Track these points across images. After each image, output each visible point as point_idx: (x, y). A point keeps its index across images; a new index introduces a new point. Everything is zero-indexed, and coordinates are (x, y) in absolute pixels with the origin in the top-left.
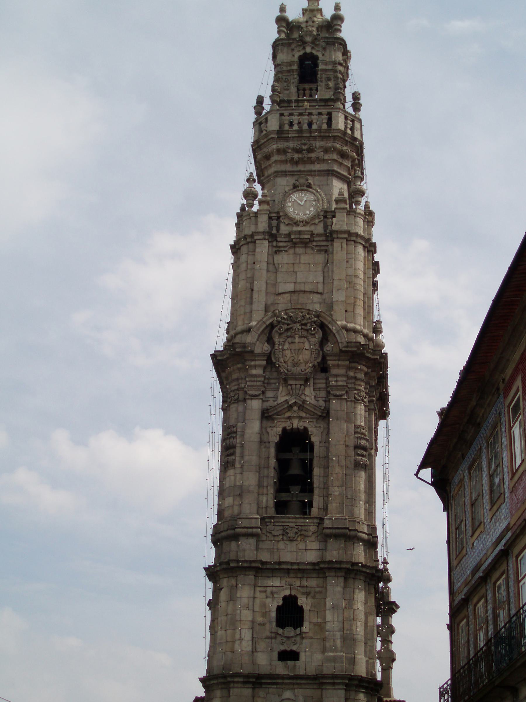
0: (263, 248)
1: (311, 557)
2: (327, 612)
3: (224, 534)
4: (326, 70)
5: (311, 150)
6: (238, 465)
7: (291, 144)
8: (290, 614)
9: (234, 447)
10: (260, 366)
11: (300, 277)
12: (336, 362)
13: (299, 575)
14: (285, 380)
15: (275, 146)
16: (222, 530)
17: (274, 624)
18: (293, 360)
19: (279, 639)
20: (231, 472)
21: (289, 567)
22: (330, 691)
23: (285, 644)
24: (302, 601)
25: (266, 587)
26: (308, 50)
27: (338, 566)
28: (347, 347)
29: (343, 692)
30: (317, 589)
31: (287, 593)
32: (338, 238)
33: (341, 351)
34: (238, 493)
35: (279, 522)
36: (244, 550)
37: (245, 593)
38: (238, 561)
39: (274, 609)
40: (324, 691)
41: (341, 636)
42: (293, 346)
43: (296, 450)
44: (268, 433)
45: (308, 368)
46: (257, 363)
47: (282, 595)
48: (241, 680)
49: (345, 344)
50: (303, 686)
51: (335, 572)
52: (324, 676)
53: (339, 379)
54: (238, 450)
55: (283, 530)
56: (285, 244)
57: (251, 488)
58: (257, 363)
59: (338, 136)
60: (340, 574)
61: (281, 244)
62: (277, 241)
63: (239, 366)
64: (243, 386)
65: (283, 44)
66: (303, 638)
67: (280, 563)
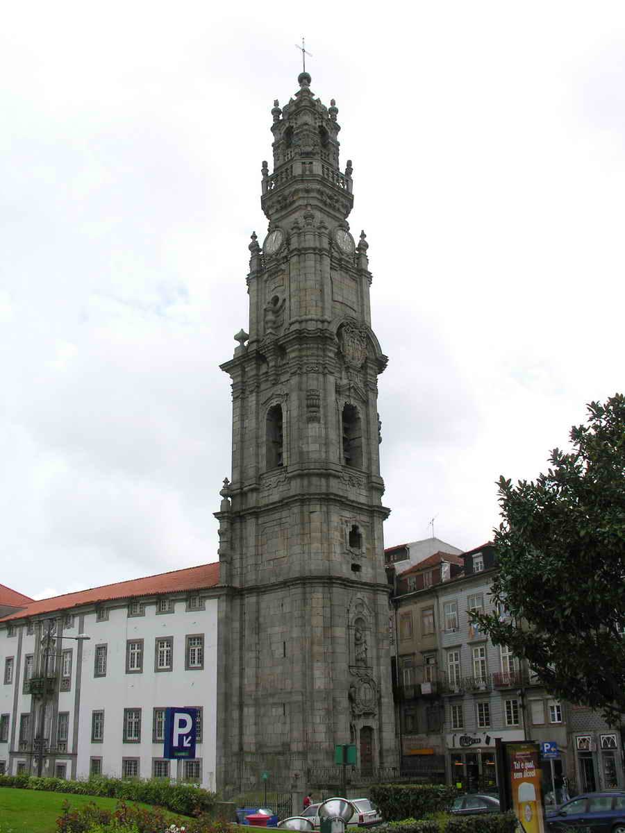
0: (327, 261)
1: (363, 500)
5: (337, 201)
6: (322, 422)
7: (327, 191)
9: (319, 407)
10: (334, 352)
12: (372, 366)
14: (347, 368)
15: (318, 187)
16: (312, 467)
20: (316, 425)
21: (357, 505)
24: (361, 530)
26: (324, 124)
31: (354, 524)
33: (377, 359)
37: (335, 519)
39: (348, 533)
45: (358, 363)
55: (350, 477)
57: (334, 441)
60: (381, 516)
61: (334, 264)
64: (321, 362)
65: (310, 111)
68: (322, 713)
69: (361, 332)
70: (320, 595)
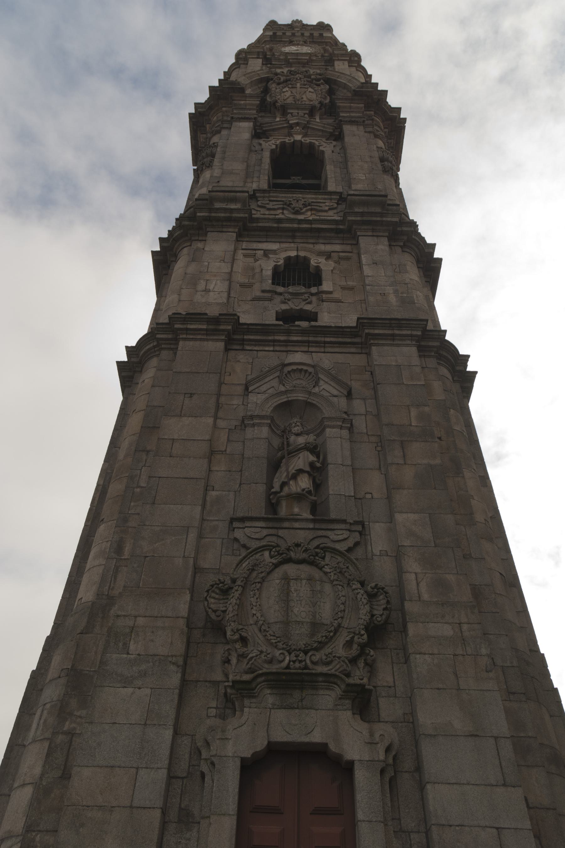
2: (365, 268)
8: (296, 274)
17: (270, 281)
18: (294, 98)
19: (278, 299)
20: (207, 175)
21: (296, 226)
22: (386, 348)
23: (290, 303)
25: (255, 250)
28: (362, 87)
29: (414, 349)
30: (341, 254)
31: (293, 254)
32: (338, 60)
34: (217, 181)
35: (277, 197)
40: (374, 348)
41: (396, 292)
42: (294, 91)
44: (260, 144)
46: (247, 102)
47: (284, 255)
48: (205, 327)
50: (327, 350)
51: (373, 230)
52: (372, 322)
54: (218, 156)
59: (330, 42)
62: (271, 64)
66: (323, 301)
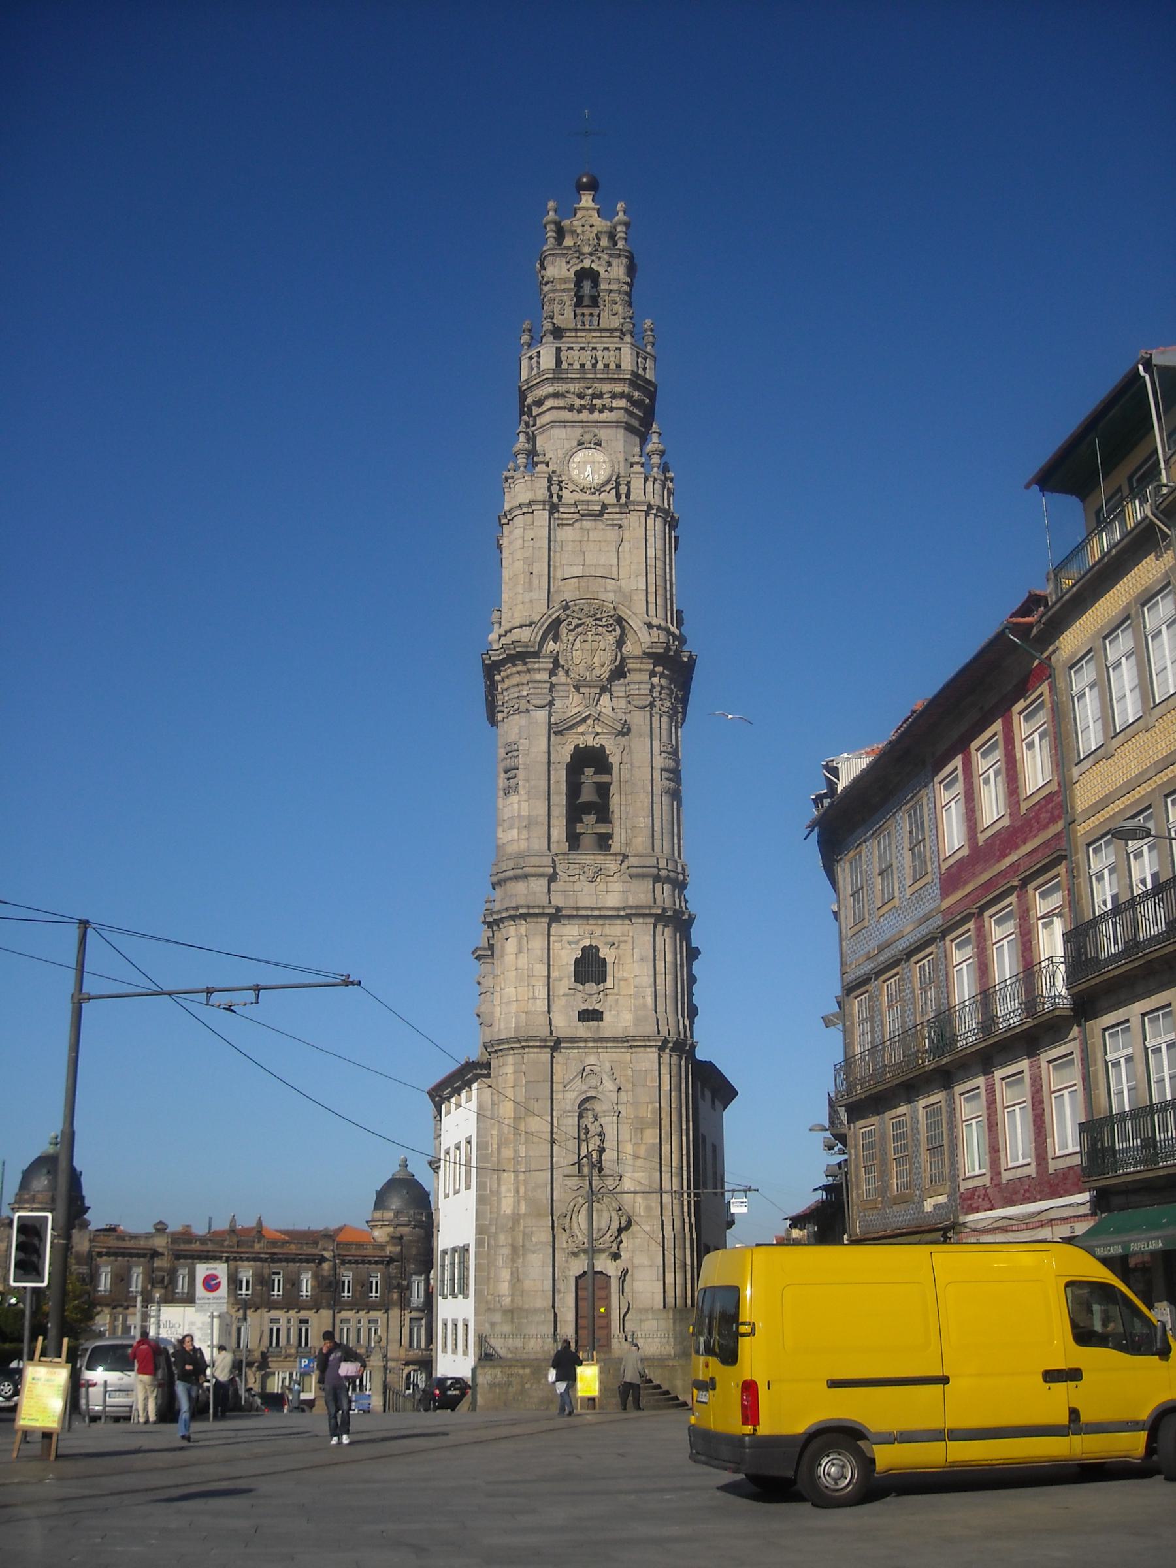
0: (542, 517)
3: (510, 874)
4: (611, 291)
6: (522, 792)
8: (590, 968)
10: (545, 669)
11: (590, 559)
13: (601, 922)
14: (577, 688)
15: (549, 389)
19: (580, 996)
20: (514, 799)
21: (589, 913)
26: (587, 264)
27: (647, 912)
30: (622, 939)
31: (587, 943)
33: (644, 653)
36: (535, 893)
38: (528, 907)
42: (587, 646)
43: (589, 771)
49: (649, 644)
52: (634, 1038)
53: (642, 686)
54: (521, 774)
56: (570, 516)
57: (540, 819)
58: (542, 665)
61: (565, 516)
63: (520, 668)
64: (525, 694)
67: (578, 909)
68: (506, 1251)
69: (600, 620)
70: (509, 1069)
